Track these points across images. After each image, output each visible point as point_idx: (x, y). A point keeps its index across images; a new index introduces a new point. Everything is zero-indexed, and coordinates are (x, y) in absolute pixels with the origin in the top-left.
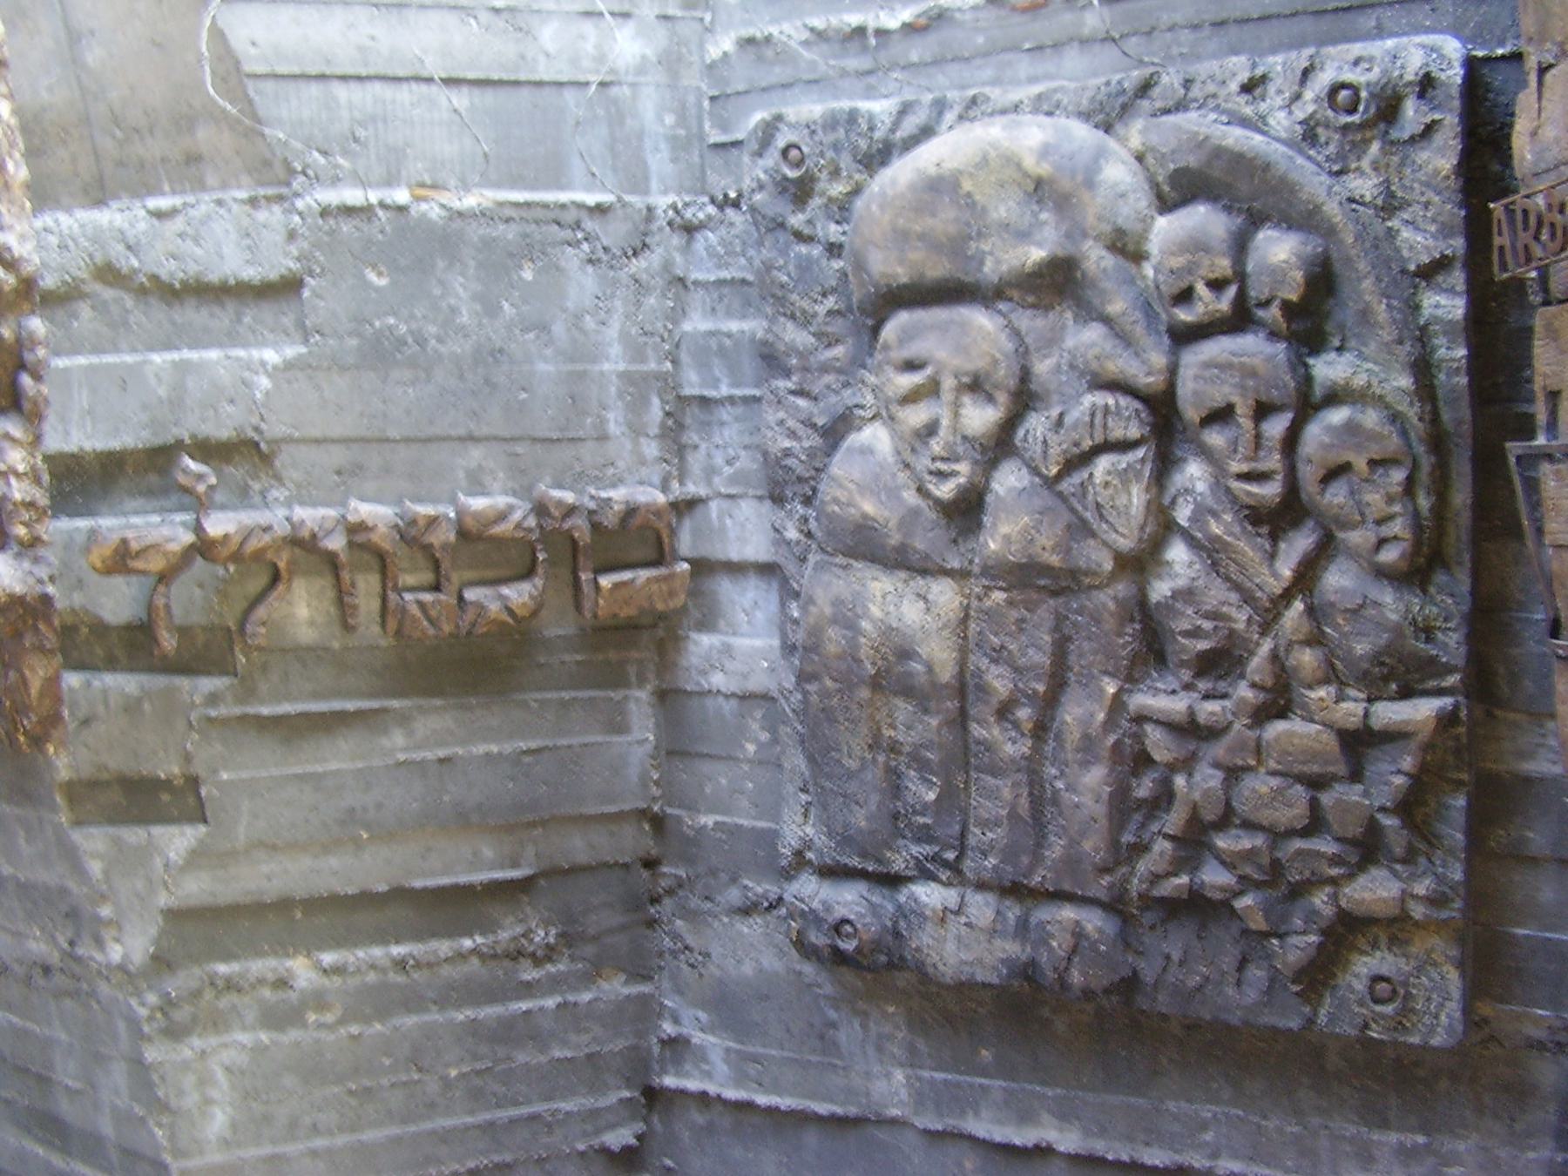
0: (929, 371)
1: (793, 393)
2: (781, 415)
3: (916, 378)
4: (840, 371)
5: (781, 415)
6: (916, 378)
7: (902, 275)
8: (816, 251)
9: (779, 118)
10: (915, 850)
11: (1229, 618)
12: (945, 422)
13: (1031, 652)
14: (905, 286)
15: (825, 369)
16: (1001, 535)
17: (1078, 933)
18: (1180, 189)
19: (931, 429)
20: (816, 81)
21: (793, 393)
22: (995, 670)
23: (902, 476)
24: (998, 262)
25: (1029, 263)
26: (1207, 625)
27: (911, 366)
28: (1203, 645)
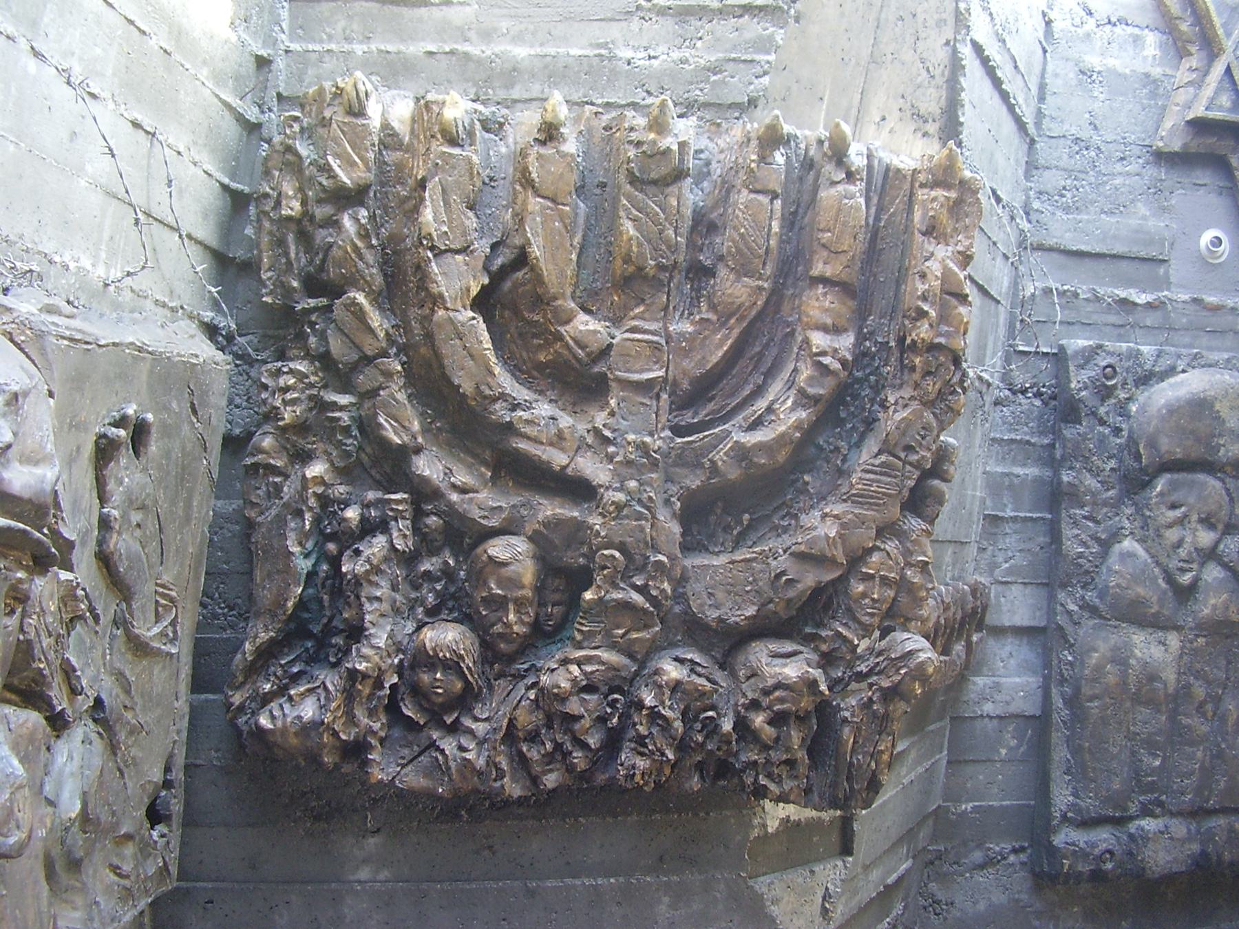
0: (1183, 509)
1: (1085, 517)
2: (1076, 532)
3: (1178, 513)
5: (1076, 532)
6: (1178, 513)
7: (1179, 453)
9: (1100, 347)
12: (1188, 539)
13: (1215, 671)
19: (1180, 544)
21: (1085, 517)
24: (1227, 451)
27: (1174, 507)
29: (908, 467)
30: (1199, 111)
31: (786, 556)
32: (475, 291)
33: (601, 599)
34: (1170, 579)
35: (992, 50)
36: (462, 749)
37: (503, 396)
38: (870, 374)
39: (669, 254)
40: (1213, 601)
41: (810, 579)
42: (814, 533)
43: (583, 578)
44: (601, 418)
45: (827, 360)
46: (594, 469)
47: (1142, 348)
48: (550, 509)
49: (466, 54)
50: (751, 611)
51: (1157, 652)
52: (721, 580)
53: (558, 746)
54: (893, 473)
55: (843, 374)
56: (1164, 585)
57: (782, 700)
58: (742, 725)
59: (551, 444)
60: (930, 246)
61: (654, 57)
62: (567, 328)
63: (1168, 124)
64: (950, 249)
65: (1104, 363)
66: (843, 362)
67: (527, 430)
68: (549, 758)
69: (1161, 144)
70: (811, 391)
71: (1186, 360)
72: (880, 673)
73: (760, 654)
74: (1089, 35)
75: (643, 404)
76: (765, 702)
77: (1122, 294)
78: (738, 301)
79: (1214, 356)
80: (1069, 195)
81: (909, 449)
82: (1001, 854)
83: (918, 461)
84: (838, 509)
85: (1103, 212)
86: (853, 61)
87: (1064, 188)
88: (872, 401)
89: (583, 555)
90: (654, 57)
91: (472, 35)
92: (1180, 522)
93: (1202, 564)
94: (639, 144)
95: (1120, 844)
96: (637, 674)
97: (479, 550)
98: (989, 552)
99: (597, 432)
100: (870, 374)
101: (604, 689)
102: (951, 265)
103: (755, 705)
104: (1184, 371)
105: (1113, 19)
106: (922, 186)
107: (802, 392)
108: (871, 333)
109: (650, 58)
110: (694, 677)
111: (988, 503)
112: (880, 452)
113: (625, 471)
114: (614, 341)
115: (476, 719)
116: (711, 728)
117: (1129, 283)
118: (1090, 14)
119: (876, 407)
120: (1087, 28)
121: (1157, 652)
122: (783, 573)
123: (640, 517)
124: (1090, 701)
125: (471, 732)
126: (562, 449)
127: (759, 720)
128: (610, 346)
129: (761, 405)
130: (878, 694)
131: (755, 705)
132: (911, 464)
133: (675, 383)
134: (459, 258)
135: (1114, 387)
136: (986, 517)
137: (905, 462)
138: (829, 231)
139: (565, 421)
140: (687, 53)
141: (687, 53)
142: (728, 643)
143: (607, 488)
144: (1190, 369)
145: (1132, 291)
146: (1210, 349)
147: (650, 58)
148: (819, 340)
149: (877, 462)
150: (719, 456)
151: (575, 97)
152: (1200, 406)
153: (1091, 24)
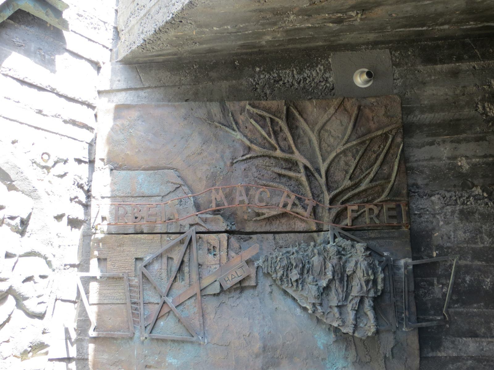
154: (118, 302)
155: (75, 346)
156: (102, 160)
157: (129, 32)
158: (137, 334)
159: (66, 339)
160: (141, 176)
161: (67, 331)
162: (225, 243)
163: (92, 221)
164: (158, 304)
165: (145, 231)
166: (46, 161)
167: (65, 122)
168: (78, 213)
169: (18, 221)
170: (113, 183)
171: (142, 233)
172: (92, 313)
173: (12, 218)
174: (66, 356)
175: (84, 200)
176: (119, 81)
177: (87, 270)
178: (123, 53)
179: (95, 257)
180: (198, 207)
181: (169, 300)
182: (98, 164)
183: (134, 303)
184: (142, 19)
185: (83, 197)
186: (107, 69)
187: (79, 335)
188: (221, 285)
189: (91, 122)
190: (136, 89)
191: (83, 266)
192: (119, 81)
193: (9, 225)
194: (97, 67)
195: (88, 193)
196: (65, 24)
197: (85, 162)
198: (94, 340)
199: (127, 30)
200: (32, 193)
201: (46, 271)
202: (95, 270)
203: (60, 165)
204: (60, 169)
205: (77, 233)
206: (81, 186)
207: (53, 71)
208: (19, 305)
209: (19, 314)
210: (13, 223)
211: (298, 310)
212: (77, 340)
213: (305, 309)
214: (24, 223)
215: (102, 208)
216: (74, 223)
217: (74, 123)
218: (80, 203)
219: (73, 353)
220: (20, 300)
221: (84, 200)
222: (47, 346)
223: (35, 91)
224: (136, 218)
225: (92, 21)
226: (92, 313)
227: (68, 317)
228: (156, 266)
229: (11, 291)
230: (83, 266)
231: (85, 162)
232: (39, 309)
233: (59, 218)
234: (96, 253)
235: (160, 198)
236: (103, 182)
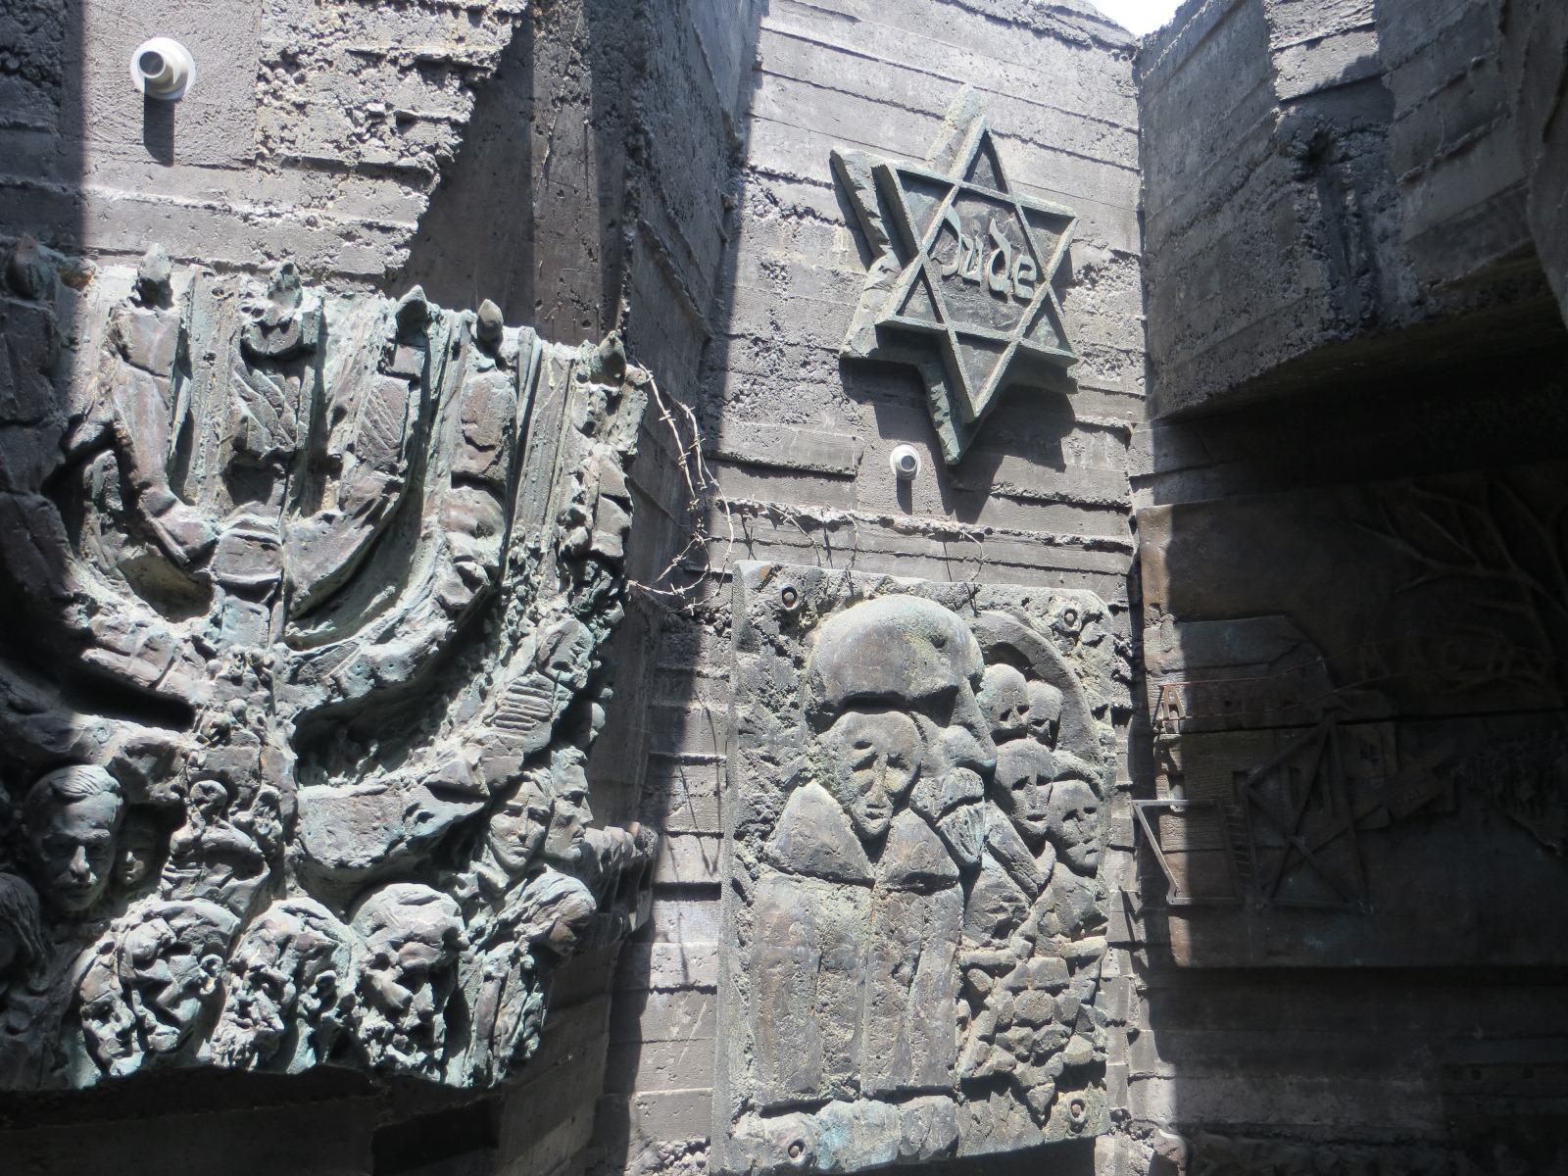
0: (871, 749)
1: (764, 758)
2: (752, 773)
4: (794, 745)
5: (752, 773)
6: (865, 752)
7: (866, 686)
8: (788, 662)
9: (779, 568)
10: (834, 1078)
11: (1017, 899)
12: (878, 782)
13: (911, 929)
14: (866, 693)
15: (785, 742)
16: (897, 858)
17: (935, 1111)
18: (999, 652)
19: (865, 788)
20: (768, 544)
21: (764, 758)
22: (892, 944)
23: (845, 818)
25: (937, 687)
26: (1006, 904)
27: (861, 745)
28: (1001, 916)
29: (560, 687)
30: (888, 314)
31: (420, 786)
32: (48, 470)
33: (197, 839)
34: (858, 828)
35: (663, 235)
36: (12, 1031)
37: (80, 598)
38: (520, 583)
39: (289, 439)
40: (905, 852)
41: (447, 812)
42: (453, 760)
43: (175, 815)
44: (199, 624)
45: (468, 566)
46: (188, 683)
47: (825, 570)
48: (130, 732)
49: (42, 191)
50: (378, 850)
51: (846, 910)
52: (339, 817)
53: (139, 1023)
54: (543, 693)
55: (487, 583)
56: (852, 833)
57: (413, 954)
58: (365, 985)
59: (140, 655)
60: (588, 443)
61: (278, 215)
62: (163, 519)
63: (855, 327)
64: (610, 448)
65: (784, 586)
66: (488, 569)
67: (107, 637)
68: (124, 1036)
69: (848, 349)
70: (452, 599)
71: (875, 584)
72: (529, 920)
73: (388, 900)
74: (772, 226)
75: (253, 611)
76: (394, 956)
77: (805, 512)
78: (369, 496)
79: (903, 582)
80: (748, 400)
81: (562, 666)
82: (673, 1152)
83: (572, 680)
84: (482, 732)
85: (783, 420)
86: (506, 239)
87: (742, 393)
88: (521, 613)
89: (175, 789)
90: (278, 215)
91: (51, 167)
92: (866, 764)
93: (895, 813)
94: (258, 312)
95: (811, 1134)
96: (240, 930)
97: (43, 782)
98: (656, 798)
99: (197, 642)
100: (520, 583)
101: (198, 948)
102: (611, 465)
103: (382, 962)
104: (871, 597)
105: (800, 210)
106: (582, 379)
107: (442, 602)
108: (522, 540)
109: (271, 215)
110: (308, 929)
111: (654, 740)
112: (529, 670)
113: (231, 687)
114: (219, 537)
115: (32, 993)
116: (327, 991)
117: (811, 499)
118: (775, 202)
119: (526, 620)
120: (771, 216)
121: (846, 910)
122: (416, 807)
123: (246, 741)
124: (772, 966)
125: (24, 1008)
126: (154, 662)
127: (385, 979)
128: (214, 543)
129: (392, 614)
130: (527, 944)
131: (382, 962)
132: (563, 683)
133: (292, 588)
134: (29, 431)
135: (795, 614)
136: (652, 757)
137: (556, 680)
138: (475, 422)
139: (159, 626)
140: (315, 213)
141: (315, 213)
142: (346, 890)
143: (207, 708)
144: (877, 595)
145: (815, 508)
146: (900, 574)
147: (271, 215)
148: (463, 543)
149: (525, 680)
150: (343, 671)
151: (179, 254)
152: (889, 636)
153: (774, 213)
154: (1208, 846)
155: (1141, 922)
156: (1156, 606)
157: (1176, 370)
158: (1249, 900)
159: (1126, 912)
160: (1227, 631)
161: (1125, 896)
162: (1392, 740)
163: (1152, 712)
164: (1280, 848)
165: (1245, 725)
166: (1071, 624)
167: (1087, 548)
168: (1123, 699)
169: (1046, 725)
170: (1184, 645)
171: (1240, 728)
172: (1175, 868)
173: (1039, 723)
174: (1128, 939)
175: (1128, 675)
176: (1166, 455)
177: (1153, 795)
178: (1166, 410)
179: (1164, 772)
180: (1335, 677)
181: (1301, 841)
182: (1149, 612)
183: (1238, 848)
184: (1200, 355)
185: (1126, 670)
186: (1144, 436)
187: (1146, 903)
188: (1390, 814)
189: (1129, 540)
190: (1198, 468)
191: (1143, 787)
192: (1166, 455)
193: (1035, 733)
194: (1123, 435)
195: (1137, 661)
196: (1072, 386)
197: (1124, 609)
198: (1179, 911)
199: (1172, 366)
200: (1060, 680)
201: (1094, 801)
202: (1169, 796)
203: (1091, 625)
204: (1090, 632)
205: (1122, 737)
206: (1120, 651)
207: (1061, 467)
208: (1062, 857)
209: (1062, 870)
210: (1040, 729)
211: (1539, 852)
212: (1143, 914)
213: (1550, 849)
214: (1055, 727)
215: (1170, 693)
216: (1120, 716)
217: (1099, 546)
218: (1122, 680)
219: (1141, 935)
220: (1062, 846)
221: (1128, 675)
222: (1105, 920)
223: (1038, 508)
224: (1228, 703)
225: (1108, 356)
226: (1175, 868)
227: (1118, 873)
228: (1271, 785)
229: (1051, 835)
230: (1143, 787)
231: (1124, 609)
232: (1090, 860)
233: (1099, 713)
234: (1165, 766)
235: (1266, 666)
236: (1163, 643)
